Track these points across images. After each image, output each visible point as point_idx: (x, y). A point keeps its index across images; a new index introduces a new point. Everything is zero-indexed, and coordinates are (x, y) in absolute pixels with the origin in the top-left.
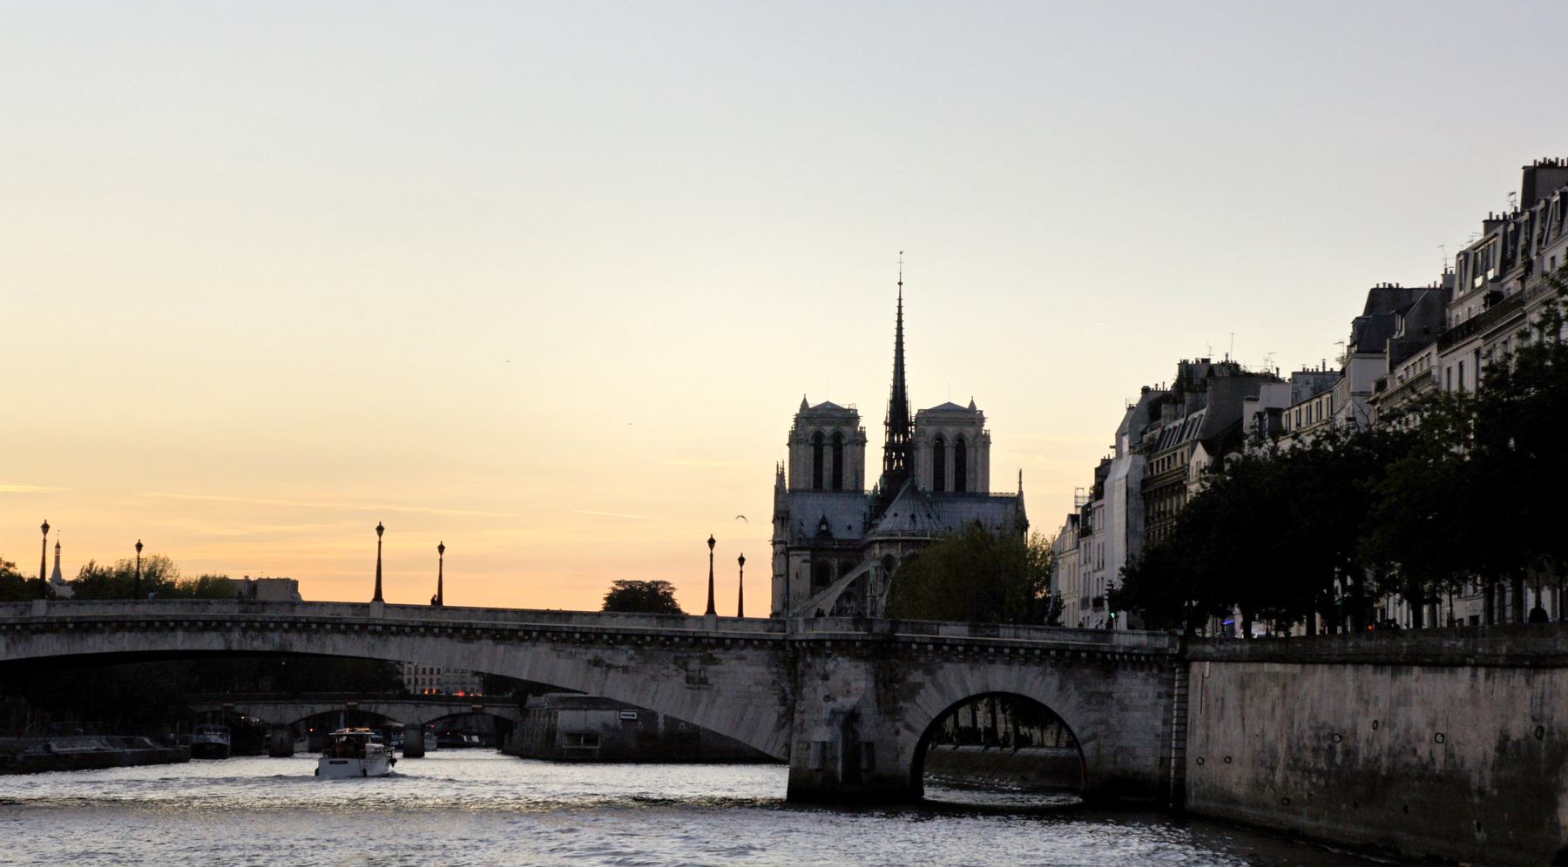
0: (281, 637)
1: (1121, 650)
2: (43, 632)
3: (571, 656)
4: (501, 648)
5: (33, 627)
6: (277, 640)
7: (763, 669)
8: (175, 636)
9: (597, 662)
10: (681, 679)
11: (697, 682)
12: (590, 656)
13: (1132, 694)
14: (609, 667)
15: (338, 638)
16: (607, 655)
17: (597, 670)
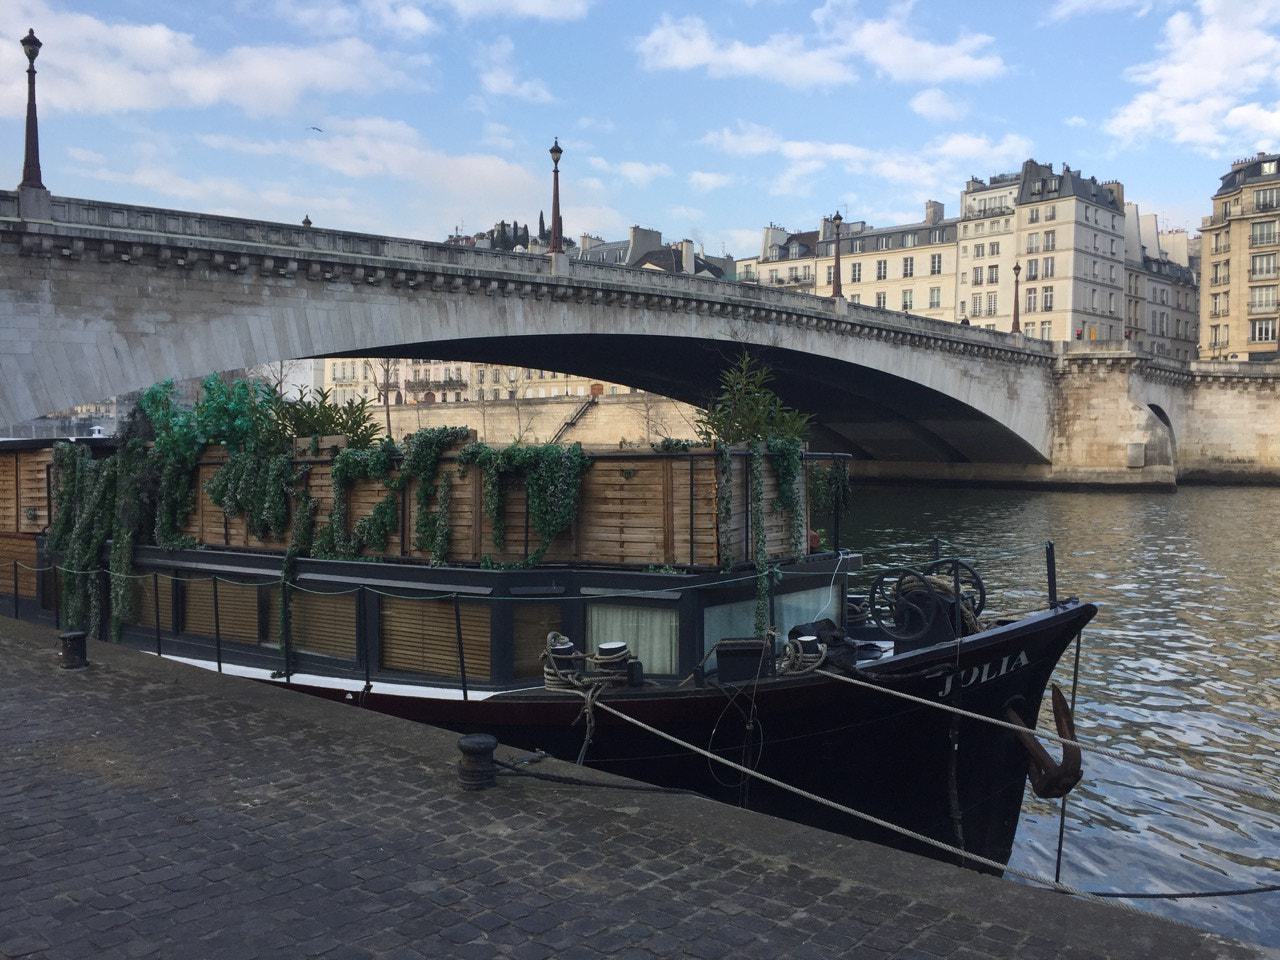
0: (774, 332)
1: (1219, 374)
2: (563, 299)
3: (954, 365)
4: (915, 354)
5: (561, 291)
6: (771, 332)
7: (1040, 383)
8: (690, 321)
9: (965, 373)
10: (1005, 390)
11: (1013, 394)
12: (961, 367)
13: (1222, 406)
14: (971, 376)
15: (813, 335)
16: (964, 363)
17: (965, 379)
